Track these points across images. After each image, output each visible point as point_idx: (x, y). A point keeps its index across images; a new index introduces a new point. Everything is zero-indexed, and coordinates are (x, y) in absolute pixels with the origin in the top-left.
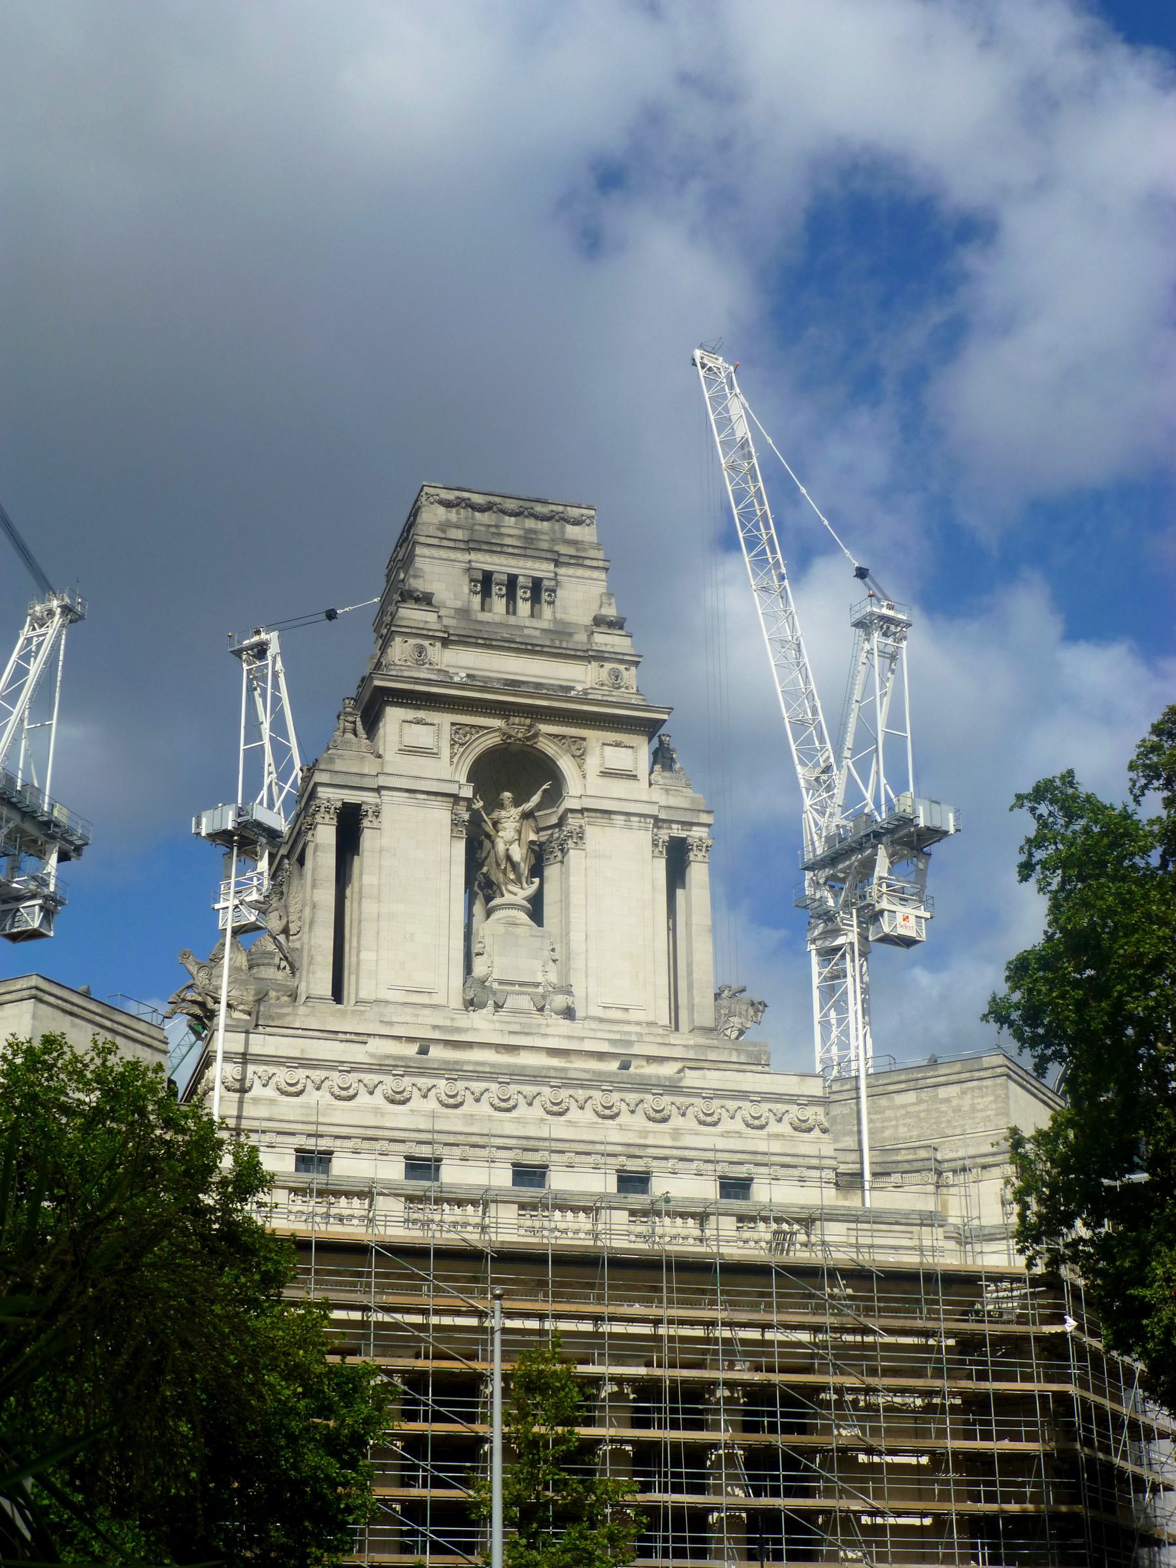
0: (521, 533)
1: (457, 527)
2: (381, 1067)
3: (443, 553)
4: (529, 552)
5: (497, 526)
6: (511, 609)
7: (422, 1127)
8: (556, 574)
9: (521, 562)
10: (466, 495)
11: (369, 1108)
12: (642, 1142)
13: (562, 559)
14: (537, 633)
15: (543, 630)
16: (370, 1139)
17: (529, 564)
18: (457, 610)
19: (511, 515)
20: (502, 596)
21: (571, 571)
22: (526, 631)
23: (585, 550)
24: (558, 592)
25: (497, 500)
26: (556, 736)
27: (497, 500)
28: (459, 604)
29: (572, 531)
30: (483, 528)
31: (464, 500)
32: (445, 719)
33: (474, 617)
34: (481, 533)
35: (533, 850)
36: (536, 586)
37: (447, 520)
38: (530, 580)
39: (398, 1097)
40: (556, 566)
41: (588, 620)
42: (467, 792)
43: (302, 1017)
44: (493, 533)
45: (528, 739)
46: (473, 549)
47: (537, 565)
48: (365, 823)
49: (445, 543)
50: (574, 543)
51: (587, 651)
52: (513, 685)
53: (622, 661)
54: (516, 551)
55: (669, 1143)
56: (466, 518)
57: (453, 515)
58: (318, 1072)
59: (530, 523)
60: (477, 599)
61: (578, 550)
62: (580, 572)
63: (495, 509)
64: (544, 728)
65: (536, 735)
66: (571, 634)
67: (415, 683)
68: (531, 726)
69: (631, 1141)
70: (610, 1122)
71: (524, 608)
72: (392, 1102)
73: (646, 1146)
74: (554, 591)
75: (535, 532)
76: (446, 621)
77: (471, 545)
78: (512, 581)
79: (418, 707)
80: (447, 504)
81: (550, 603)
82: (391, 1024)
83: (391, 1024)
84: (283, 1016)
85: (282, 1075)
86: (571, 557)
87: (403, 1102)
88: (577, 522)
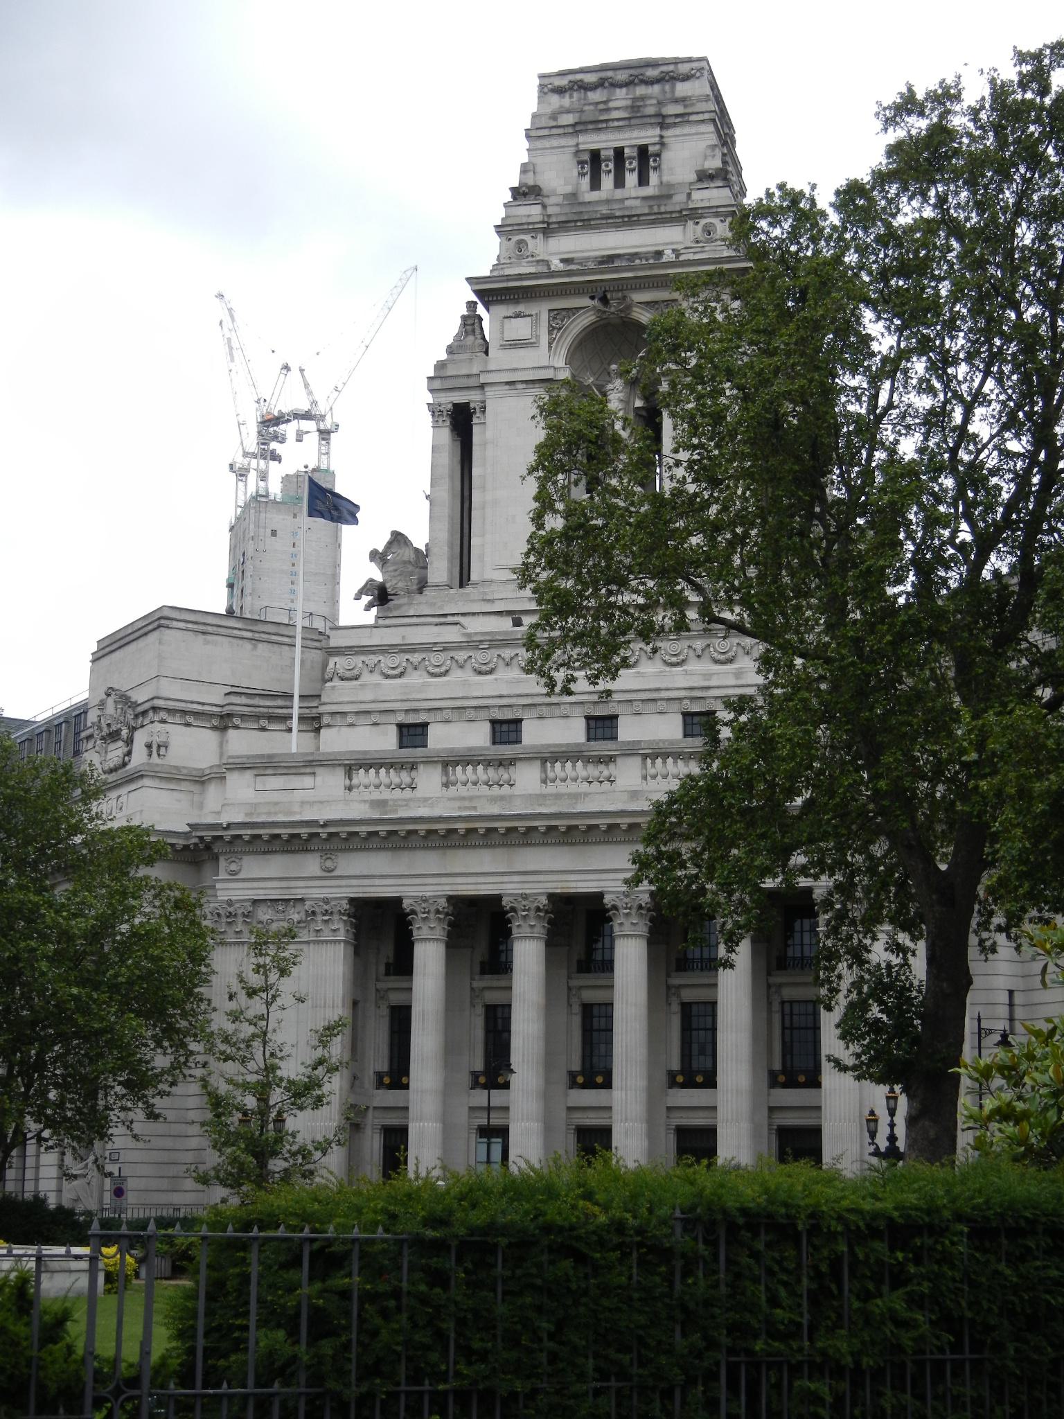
0: (629, 103)
1: (568, 112)
2: (472, 644)
3: (555, 142)
4: (633, 122)
5: (605, 102)
6: (619, 183)
7: (505, 693)
8: (661, 137)
9: (627, 135)
10: (579, 77)
11: (462, 683)
12: (706, 684)
13: (669, 121)
14: (638, 203)
15: (645, 198)
16: (460, 711)
17: (635, 134)
18: (565, 196)
19: (621, 86)
20: (609, 171)
21: (678, 131)
22: (627, 203)
23: (693, 105)
24: (664, 155)
25: (610, 74)
26: (647, 303)
27: (610, 74)
28: (569, 189)
29: (682, 89)
30: (592, 107)
31: (575, 82)
32: (542, 310)
33: (581, 200)
34: (590, 113)
35: (641, 416)
36: (643, 152)
37: (561, 107)
38: (636, 149)
39: (484, 668)
40: (661, 128)
41: (693, 177)
42: (565, 374)
43: (422, 605)
44: (601, 110)
45: (621, 311)
46: (580, 131)
47: (642, 133)
48: (475, 420)
49: (555, 131)
50: (683, 100)
51: (680, 212)
52: (608, 260)
53: (717, 215)
54: (621, 123)
55: (733, 682)
56: (579, 100)
57: (566, 101)
58: (416, 655)
59: (641, 90)
60: (587, 179)
61: (685, 106)
62: (687, 130)
63: (607, 84)
64: (638, 297)
65: (629, 308)
66: (670, 197)
67: (508, 280)
68: (624, 298)
69: (695, 685)
70: (679, 669)
71: (631, 179)
72: (480, 673)
73: (708, 688)
74: (658, 155)
75: (643, 98)
76: (550, 210)
77: (579, 128)
78: (619, 152)
79: (516, 301)
80: (560, 91)
81: (655, 168)
82: (492, 601)
83: (492, 601)
84: (399, 606)
85: (387, 662)
86: (677, 116)
87: (491, 672)
88: (687, 78)
